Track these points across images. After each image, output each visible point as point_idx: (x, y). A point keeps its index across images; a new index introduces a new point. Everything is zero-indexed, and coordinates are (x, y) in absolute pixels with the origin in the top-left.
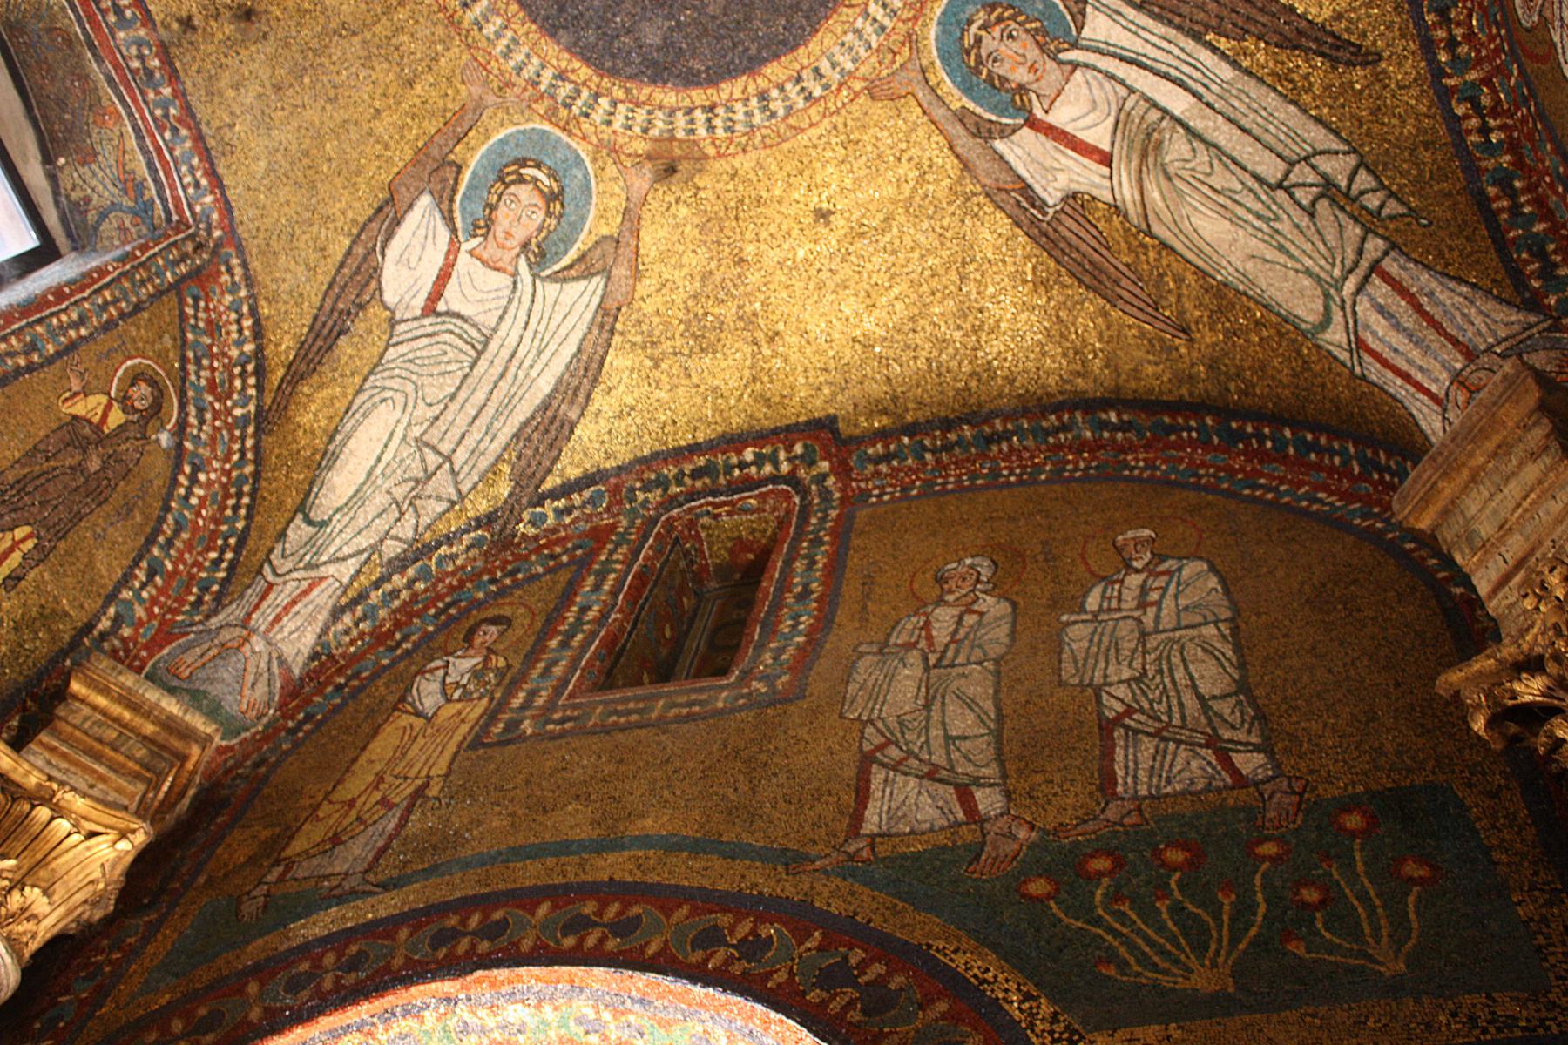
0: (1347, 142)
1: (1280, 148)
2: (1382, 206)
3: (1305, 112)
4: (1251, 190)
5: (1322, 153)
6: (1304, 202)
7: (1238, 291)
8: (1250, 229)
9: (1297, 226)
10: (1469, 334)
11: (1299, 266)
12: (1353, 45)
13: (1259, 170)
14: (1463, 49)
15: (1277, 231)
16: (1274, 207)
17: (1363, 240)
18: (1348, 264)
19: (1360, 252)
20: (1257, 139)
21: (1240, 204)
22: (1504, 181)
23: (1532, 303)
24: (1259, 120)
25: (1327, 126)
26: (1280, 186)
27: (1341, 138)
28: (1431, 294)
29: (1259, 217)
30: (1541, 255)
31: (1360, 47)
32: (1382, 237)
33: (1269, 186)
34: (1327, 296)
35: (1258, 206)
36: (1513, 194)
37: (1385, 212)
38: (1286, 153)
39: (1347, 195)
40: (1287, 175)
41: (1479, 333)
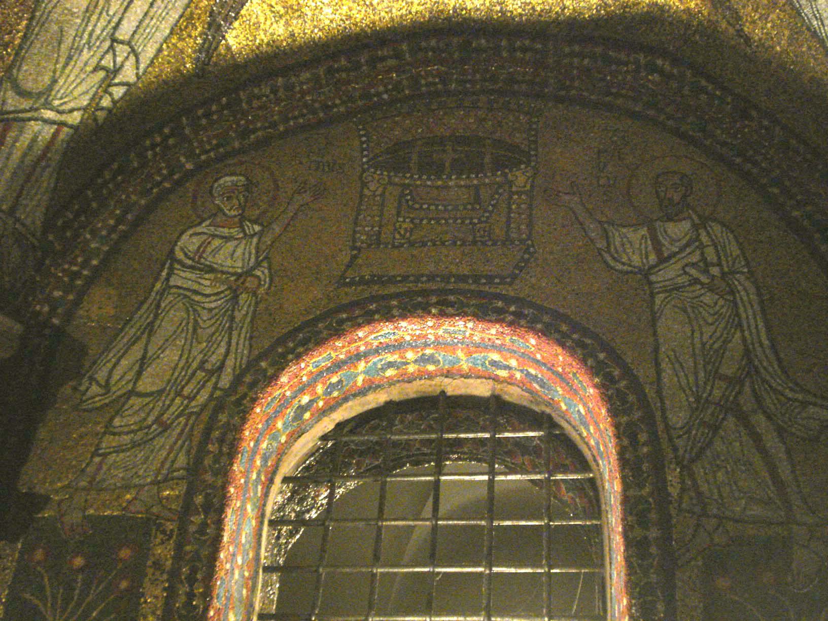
0: (145, 72)
1: (141, 30)
2: (102, 109)
3: (165, 41)
4: (109, 22)
5: (137, 61)
6: (103, 63)
7: (34, 11)
8: (81, 29)
9: (86, 64)
10: (24, 202)
11: (58, 74)
12: (209, 60)
13: (125, 22)
14: (204, 121)
15: (82, 51)
16: (98, 44)
17: (78, 109)
18: (61, 108)
19: (71, 111)
20: (146, 14)
21: (99, 19)
22: (120, 171)
23: (48, 226)
24: (160, 11)
25: (156, 56)
26: (114, 40)
27: (148, 67)
28: (48, 166)
29: (91, 35)
30: (77, 215)
31: (208, 64)
32: (82, 119)
33: (113, 34)
34: (40, 95)
35: (98, 32)
36: (114, 178)
37: (99, 113)
38: (137, 36)
39: (110, 85)
40: (122, 42)
41: (26, 206)
